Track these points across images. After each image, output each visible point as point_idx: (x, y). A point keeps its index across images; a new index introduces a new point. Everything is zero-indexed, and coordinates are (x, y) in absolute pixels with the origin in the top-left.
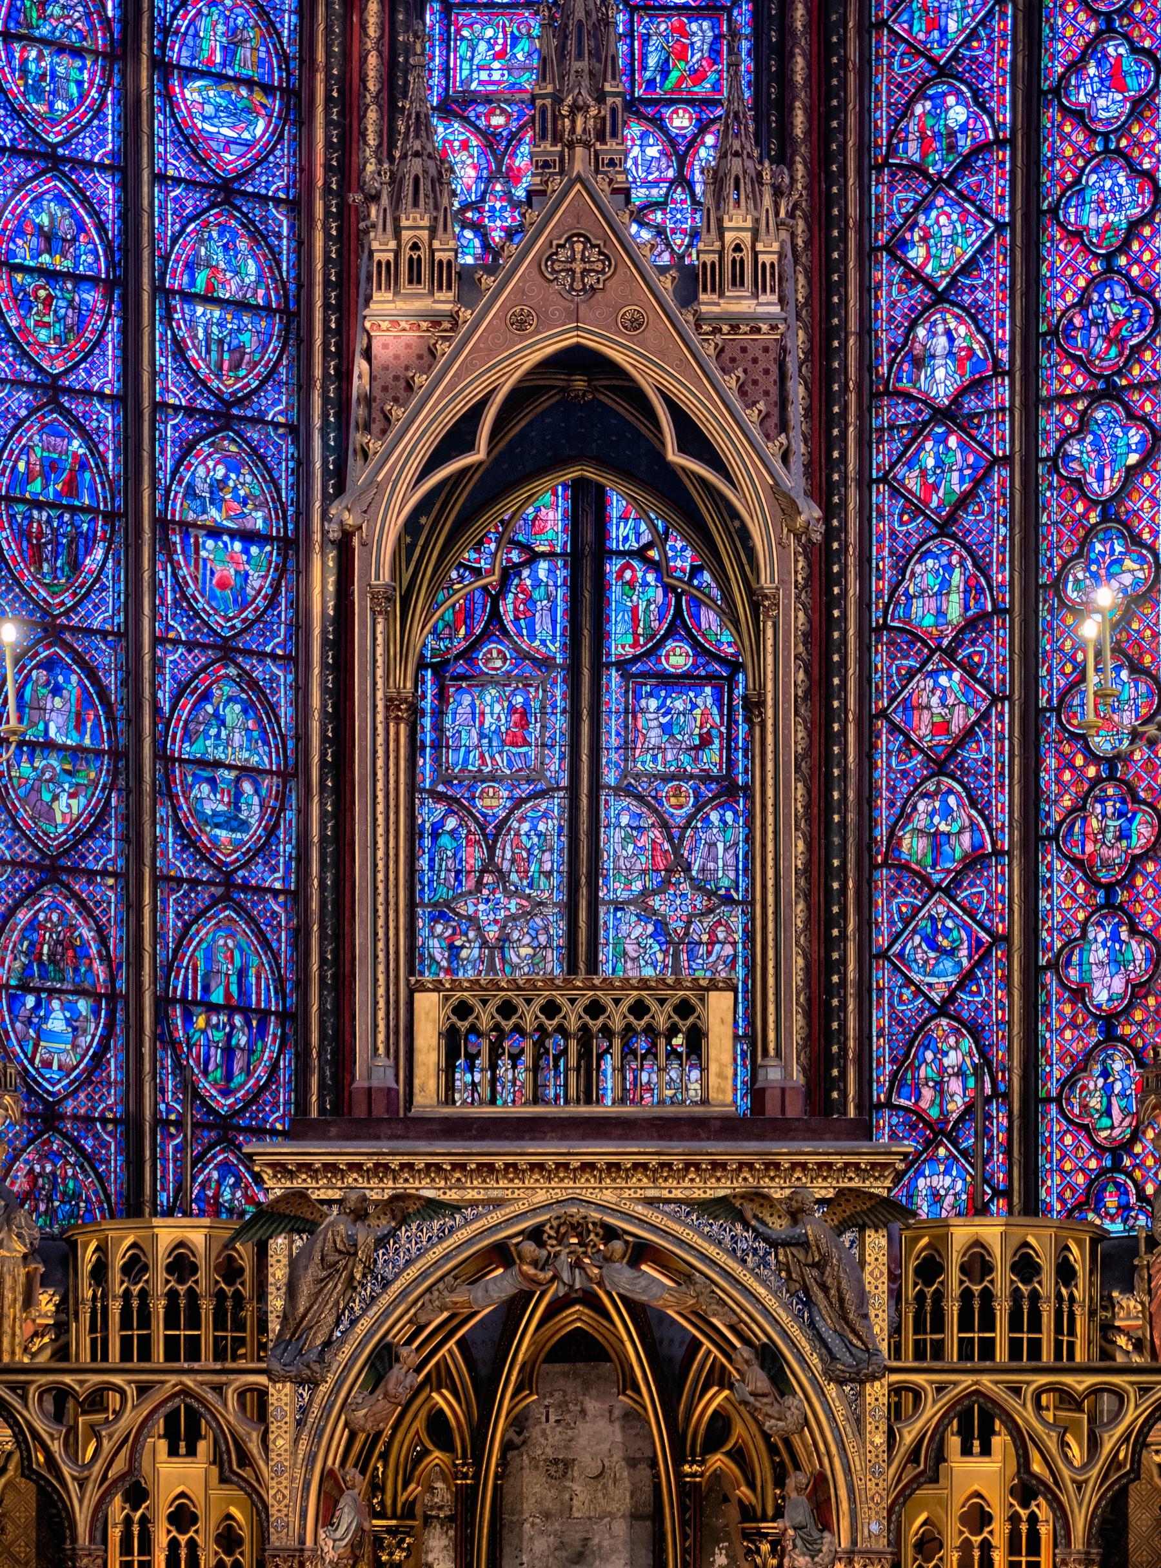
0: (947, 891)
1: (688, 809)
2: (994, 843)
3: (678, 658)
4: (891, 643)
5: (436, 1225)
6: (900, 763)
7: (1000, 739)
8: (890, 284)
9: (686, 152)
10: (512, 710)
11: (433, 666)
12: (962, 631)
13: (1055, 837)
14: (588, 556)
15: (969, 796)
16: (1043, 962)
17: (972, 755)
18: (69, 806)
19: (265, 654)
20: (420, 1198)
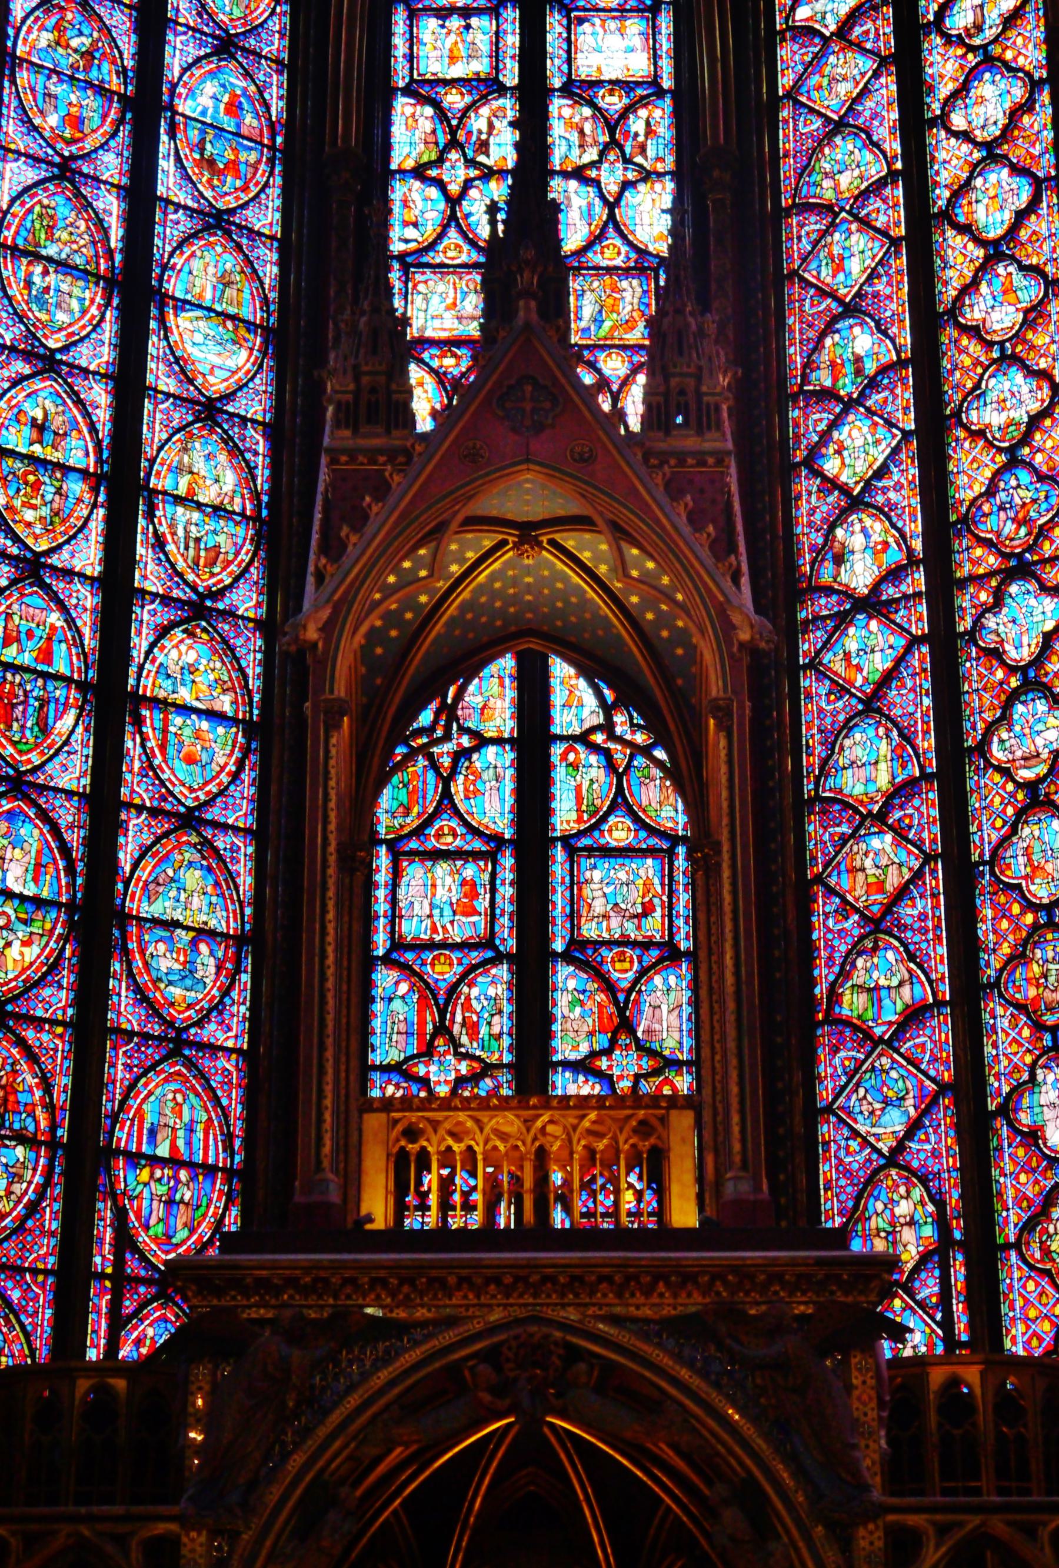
0: (889, 1043)
1: (630, 975)
2: (935, 994)
3: (619, 832)
4: (824, 812)
5: (381, 1346)
6: (837, 922)
7: (934, 896)
8: (810, 494)
9: (620, 391)
10: (464, 883)
12: (889, 797)
13: (997, 984)
14: (533, 742)
15: (907, 950)
16: (992, 1107)
17: (908, 912)
18: (22, 954)
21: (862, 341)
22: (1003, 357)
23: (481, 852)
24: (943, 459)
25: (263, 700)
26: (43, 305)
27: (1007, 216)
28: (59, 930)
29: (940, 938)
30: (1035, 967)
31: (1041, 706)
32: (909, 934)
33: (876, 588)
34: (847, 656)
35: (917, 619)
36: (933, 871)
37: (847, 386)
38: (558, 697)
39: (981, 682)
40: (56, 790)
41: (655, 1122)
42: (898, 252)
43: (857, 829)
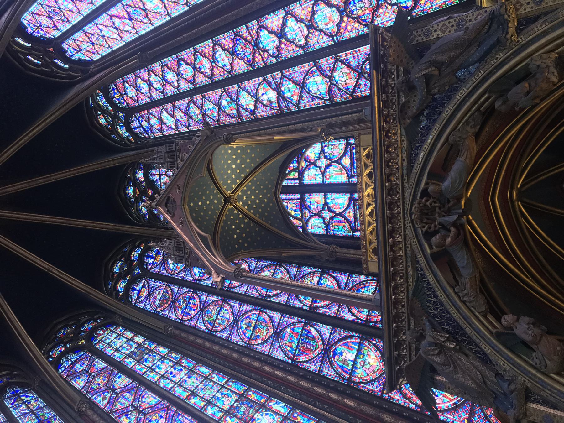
7: (347, 55)
11: (353, 233)
14: (326, 188)
17: (354, 63)
18: (373, 359)
19: (346, 283)
20: (412, 300)
21: (224, 103)
22: (214, 62)
23: (354, 204)
24: (240, 75)
25: (317, 268)
26: (223, 322)
27: (187, 66)
28: (367, 344)
29: (359, 50)
30: (359, 13)
31: (286, 30)
32: (360, 62)
33: (274, 90)
34: (292, 96)
35: (278, 75)
36: (341, 56)
37: (234, 106)
38: (313, 182)
39: (289, 52)
40: (329, 338)
41: (367, 151)
42: (205, 95)
43: (334, 85)
